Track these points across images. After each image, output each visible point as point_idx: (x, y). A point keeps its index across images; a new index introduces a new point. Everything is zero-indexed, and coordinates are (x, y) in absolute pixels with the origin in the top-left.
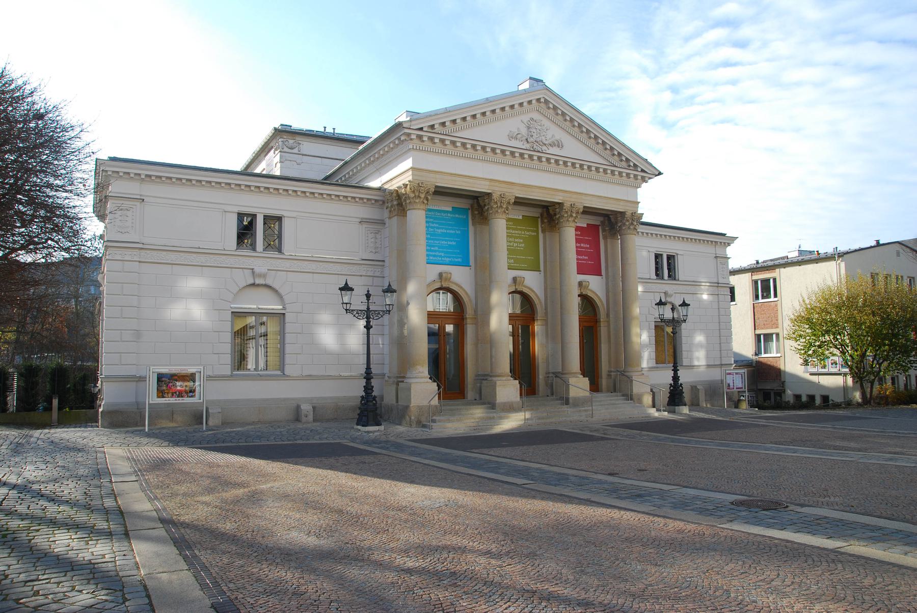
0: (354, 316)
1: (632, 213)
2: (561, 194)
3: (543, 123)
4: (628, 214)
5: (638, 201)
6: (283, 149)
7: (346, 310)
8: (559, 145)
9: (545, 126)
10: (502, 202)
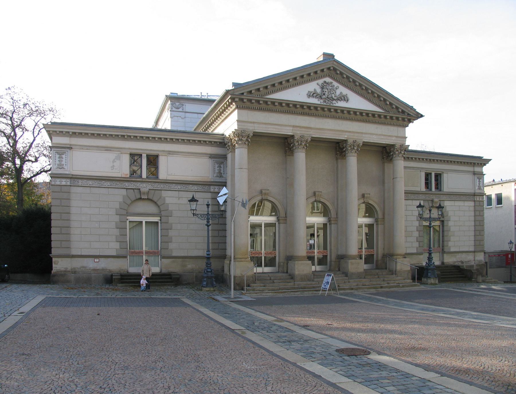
0: (199, 218)
1: (401, 146)
2: (347, 134)
3: (333, 84)
4: (397, 146)
5: (406, 136)
6: (172, 109)
7: (193, 214)
8: (345, 98)
9: (335, 87)
10: (301, 141)
